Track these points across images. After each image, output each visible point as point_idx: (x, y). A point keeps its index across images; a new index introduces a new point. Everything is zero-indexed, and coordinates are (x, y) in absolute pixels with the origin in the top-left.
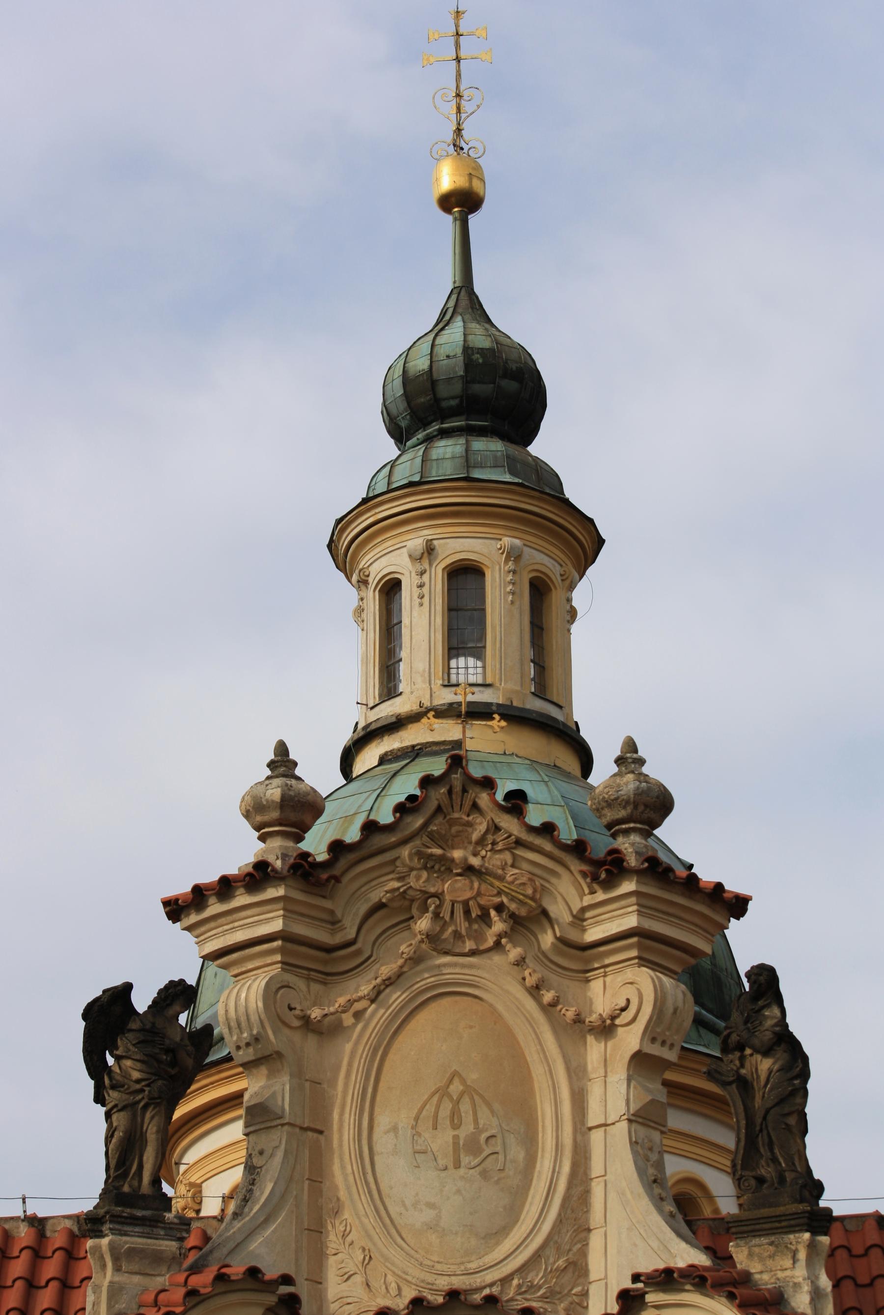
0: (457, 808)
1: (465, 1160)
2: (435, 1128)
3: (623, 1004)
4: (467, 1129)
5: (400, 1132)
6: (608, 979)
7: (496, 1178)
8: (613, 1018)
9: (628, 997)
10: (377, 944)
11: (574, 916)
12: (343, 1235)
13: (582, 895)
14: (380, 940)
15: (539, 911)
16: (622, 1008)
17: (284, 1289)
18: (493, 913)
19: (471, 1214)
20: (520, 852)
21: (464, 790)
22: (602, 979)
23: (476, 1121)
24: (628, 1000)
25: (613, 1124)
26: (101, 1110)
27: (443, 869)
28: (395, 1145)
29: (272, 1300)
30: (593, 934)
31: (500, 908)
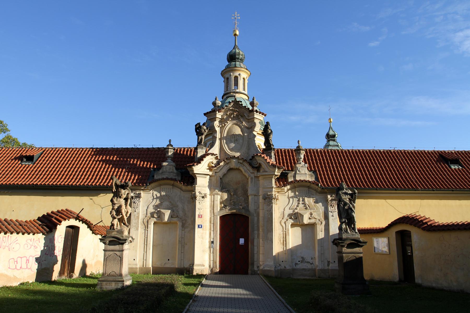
4: (236, 138)
17: (216, 155)
20: (242, 109)
21: (236, 102)
26: (197, 136)
29: (215, 156)
31: (240, 115)
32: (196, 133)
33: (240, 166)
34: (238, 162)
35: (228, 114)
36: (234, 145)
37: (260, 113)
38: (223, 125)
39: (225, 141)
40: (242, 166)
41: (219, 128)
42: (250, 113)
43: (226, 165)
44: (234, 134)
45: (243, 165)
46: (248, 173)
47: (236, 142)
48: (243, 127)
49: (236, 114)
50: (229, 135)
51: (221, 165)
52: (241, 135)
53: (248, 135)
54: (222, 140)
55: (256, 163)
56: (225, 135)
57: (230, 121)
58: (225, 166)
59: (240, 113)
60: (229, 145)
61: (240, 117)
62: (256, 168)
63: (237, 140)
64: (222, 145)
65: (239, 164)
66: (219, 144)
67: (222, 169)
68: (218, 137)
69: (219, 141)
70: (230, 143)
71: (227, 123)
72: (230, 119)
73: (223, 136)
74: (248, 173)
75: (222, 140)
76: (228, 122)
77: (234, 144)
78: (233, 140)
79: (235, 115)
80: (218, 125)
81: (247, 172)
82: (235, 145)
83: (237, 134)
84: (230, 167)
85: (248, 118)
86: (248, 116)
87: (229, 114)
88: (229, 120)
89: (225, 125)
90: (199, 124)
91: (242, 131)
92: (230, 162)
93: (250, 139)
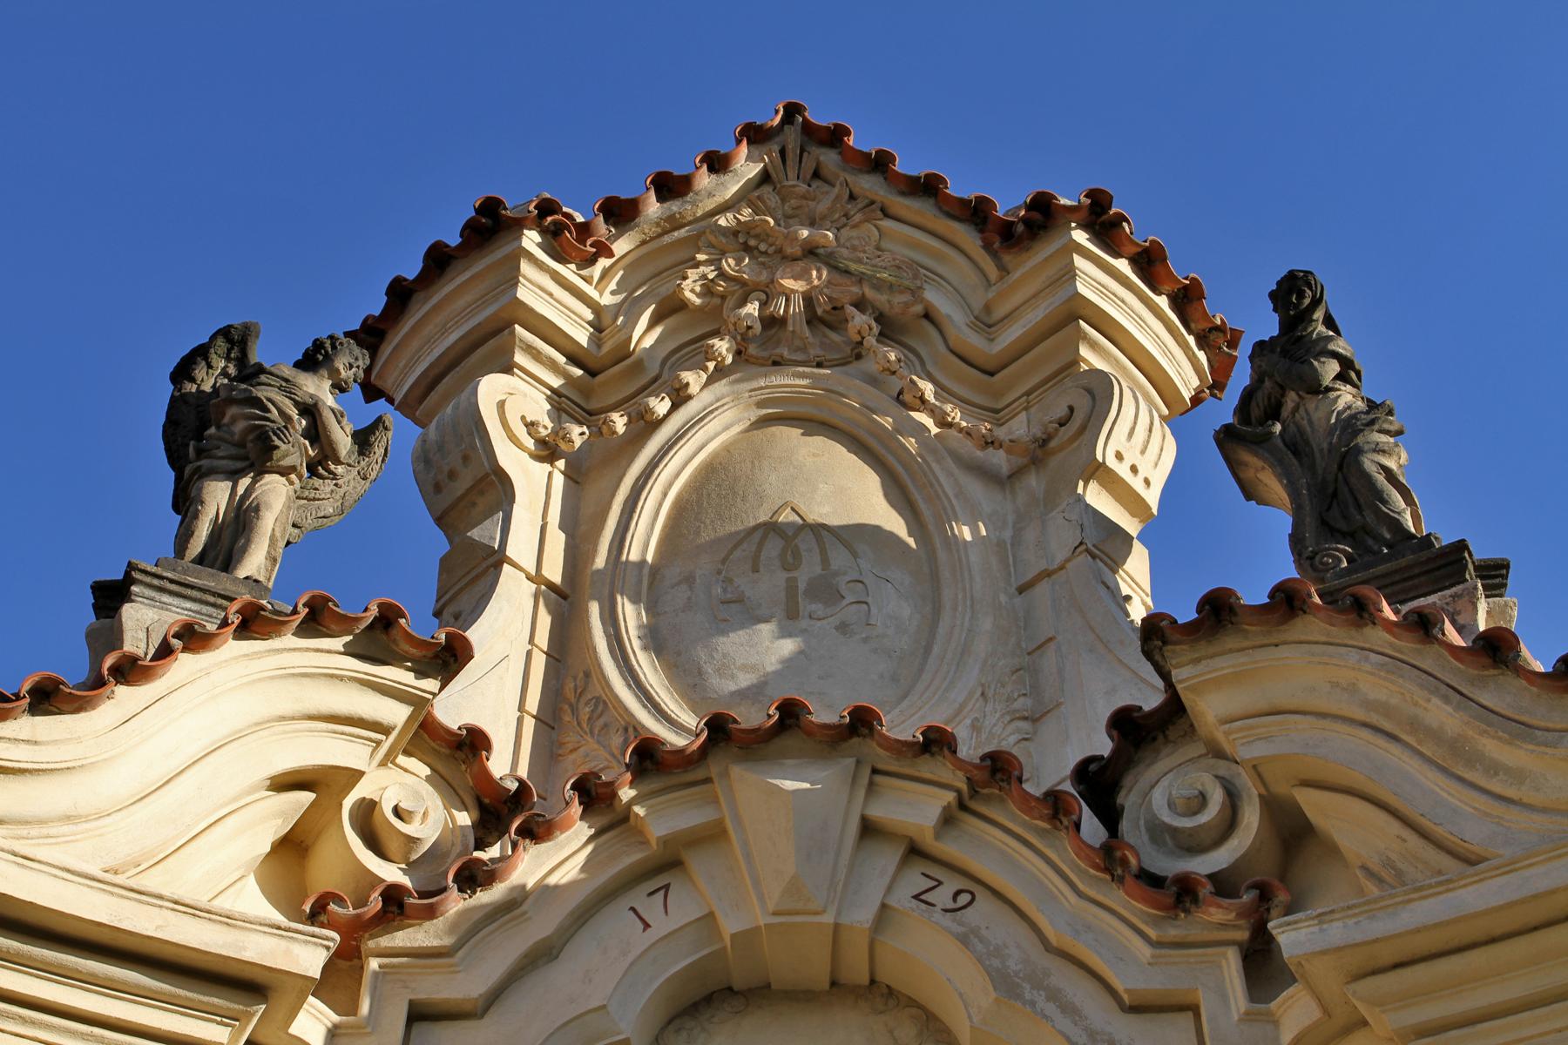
0: (792, 174)
1: (806, 606)
2: (755, 570)
3: (1062, 411)
4: (809, 570)
5: (698, 581)
6: (1033, 410)
7: (864, 636)
8: (1044, 443)
9: (1071, 403)
10: (669, 364)
11: (976, 318)
12: (589, 719)
13: (989, 284)
14: (673, 359)
15: (918, 309)
16: (1060, 418)
18: (851, 310)
19: (820, 678)
20: (887, 224)
21: (802, 150)
22: (1024, 413)
23: (825, 561)
24: (1071, 409)
25: (1062, 568)
27: (771, 250)
28: (689, 598)
30: (1011, 335)
31: (860, 305)
32: (172, 474)
33: (902, 898)
34: (869, 830)
35: (691, 289)
36: (788, 646)
37: (1149, 264)
38: (619, 422)
39: (631, 615)
40: (942, 896)
41: (559, 480)
42: (1004, 270)
43: (638, 898)
44: (786, 517)
45: (951, 884)
46: (1069, 1010)
47: (818, 608)
48: (911, 444)
49: (809, 300)
50: (706, 536)
51: (545, 892)
52: (891, 536)
53: (1003, 549)
54: (594, 609)
55: (1202, 800)
56: (644, 543)
57: (720, 372)
58: (617, 922)
59: (860, 279)
60: (702, 655)
61: (860, 321)
62: (1223, 884)
63: (826, 591)
64: (592, 672)
65: (886, 859)
66: (539, 663)
67: (542, 955)
68: (521, 546)
69: (545, 620)
70: (724, 633)
71: (680, 397)
72: (722, 346)
73: (600, 561)
74: (1069, 1010)
75: (594, 609)
76: (693, 379)
77: (785, 633)
78: (770, 583)
79: (798, 306)
80: (531, 426)
81: (1054, 996)
82: (801, 652)
83: (834, 521)
84: (709, 920)
85: (974, 341)
86: (986, 323)
87: (708, 290)
88: (709, 354)
89: (645, 425)
90: (236, 339)
91: (898, 492)
92: (712, 836)
93: (1043, 590)
